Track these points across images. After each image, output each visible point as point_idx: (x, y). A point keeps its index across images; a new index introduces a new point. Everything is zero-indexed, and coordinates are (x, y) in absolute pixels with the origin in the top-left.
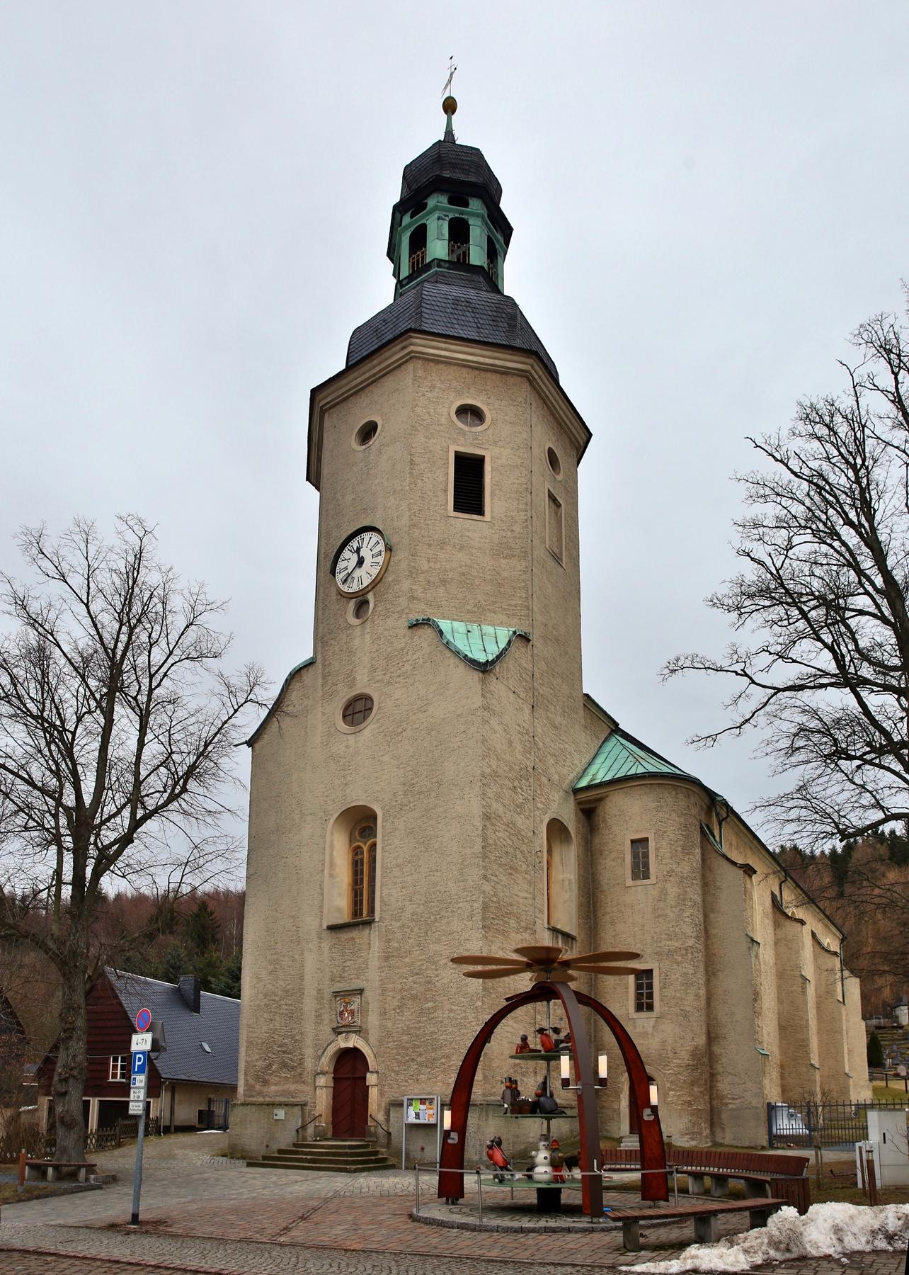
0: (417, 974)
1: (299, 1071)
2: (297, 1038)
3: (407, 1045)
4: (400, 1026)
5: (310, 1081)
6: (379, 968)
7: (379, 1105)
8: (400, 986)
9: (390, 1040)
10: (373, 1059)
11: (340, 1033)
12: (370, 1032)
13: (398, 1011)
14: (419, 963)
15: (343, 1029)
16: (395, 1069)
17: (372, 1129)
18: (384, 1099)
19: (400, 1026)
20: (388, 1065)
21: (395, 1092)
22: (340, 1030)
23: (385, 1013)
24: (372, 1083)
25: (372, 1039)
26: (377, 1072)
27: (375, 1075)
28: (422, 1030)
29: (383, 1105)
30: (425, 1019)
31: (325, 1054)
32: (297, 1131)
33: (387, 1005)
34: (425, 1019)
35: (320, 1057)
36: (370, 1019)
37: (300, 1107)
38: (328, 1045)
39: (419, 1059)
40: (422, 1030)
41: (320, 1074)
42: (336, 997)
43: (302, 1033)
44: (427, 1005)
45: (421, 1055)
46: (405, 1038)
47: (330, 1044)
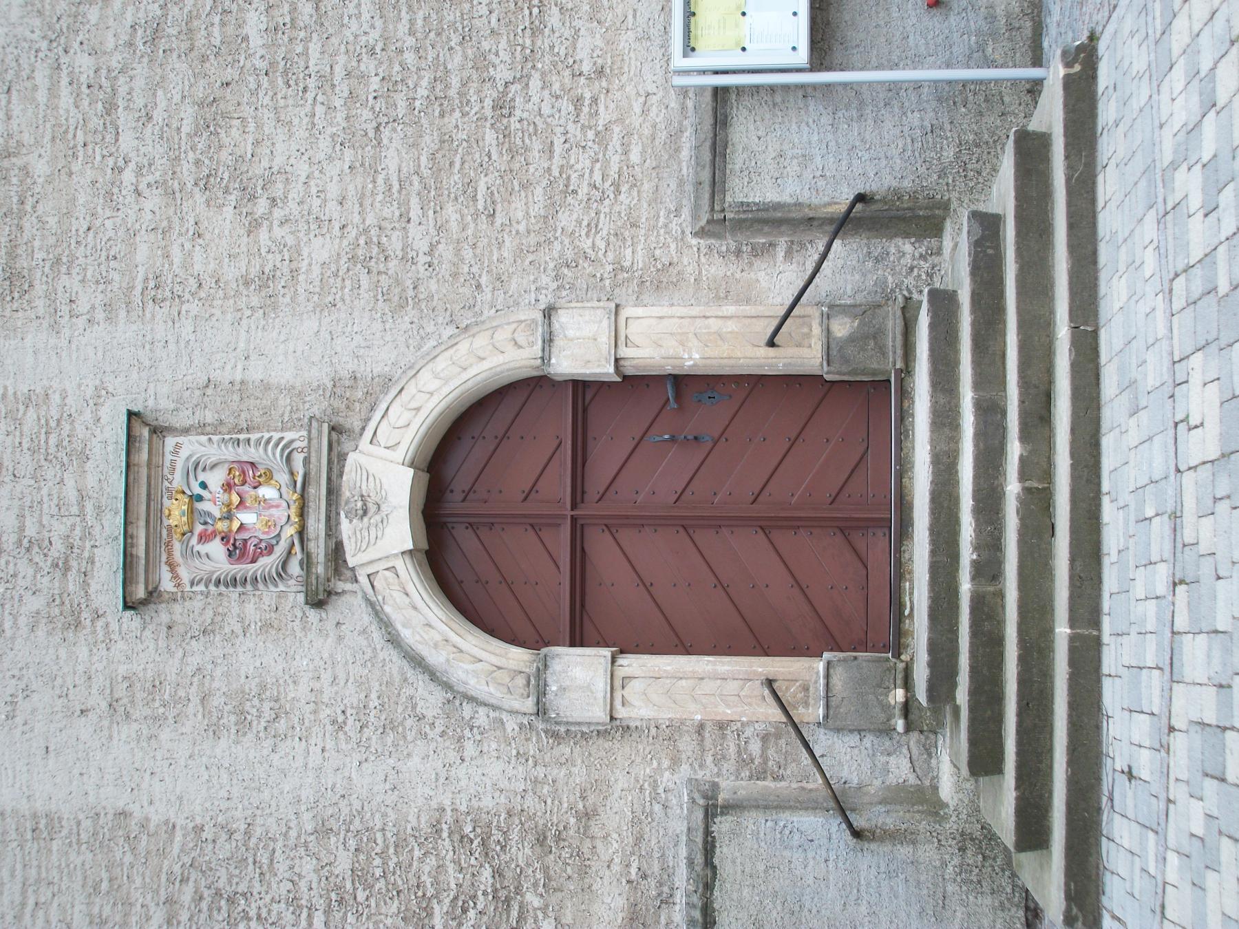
0: (110, 107)
1: (521, 852)
2: (344, 863)
3: (429, 141)
4: (333, 190)
5: (579, 774)
6: (55, 328)
7: (722, 293)
8: (154, 200)
9: (394, 244)
10: (481, 341)
11: (337, 553)
12: (347, 366)
13: (262, 206)
14: (65, 99)
15: (316, 526)
16: (537, 209)
17: (842, 328)
18: (688, 263)
19: (333, 190)
20: (520, 252)
21: (655, 200)
22: (319, 549)
23: (266, 279)
24: (605, 339)
25: (379, 361)
26: (549, 313)
27: (563, 319)
28: (368, 65)
29: (716, 268)
30: (314, 48)
31: (436, 658)
32: (857, 834)
33: (231, 273)
34: (314, 48)
35: (456, 696)
36: (283, 374)
37: (722, 825)
38: (394, 640)
39: (502, 74)
40: (368, 65)
41: (541, 710)
42: (153, 595)
43: (323, 831)
44: (256, 41)
45: (481, 62)
46: (394, 159)
47: (385, 623)
